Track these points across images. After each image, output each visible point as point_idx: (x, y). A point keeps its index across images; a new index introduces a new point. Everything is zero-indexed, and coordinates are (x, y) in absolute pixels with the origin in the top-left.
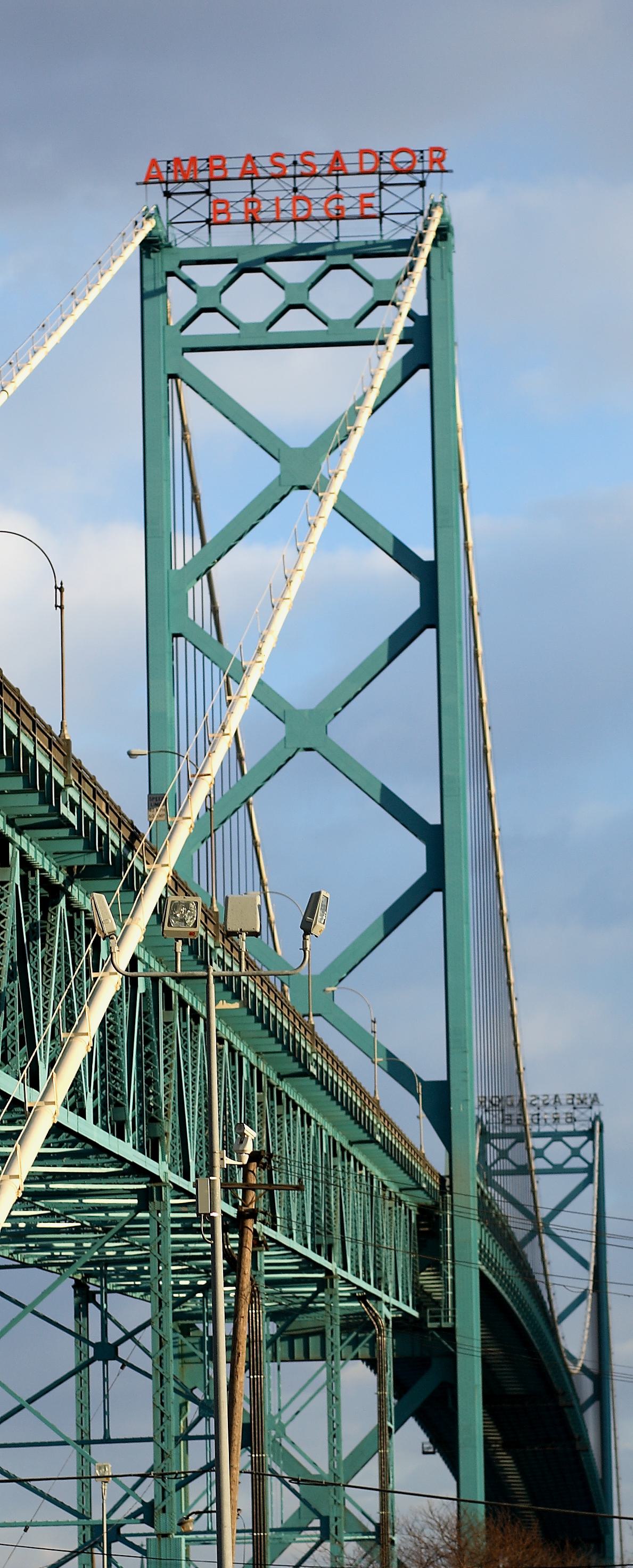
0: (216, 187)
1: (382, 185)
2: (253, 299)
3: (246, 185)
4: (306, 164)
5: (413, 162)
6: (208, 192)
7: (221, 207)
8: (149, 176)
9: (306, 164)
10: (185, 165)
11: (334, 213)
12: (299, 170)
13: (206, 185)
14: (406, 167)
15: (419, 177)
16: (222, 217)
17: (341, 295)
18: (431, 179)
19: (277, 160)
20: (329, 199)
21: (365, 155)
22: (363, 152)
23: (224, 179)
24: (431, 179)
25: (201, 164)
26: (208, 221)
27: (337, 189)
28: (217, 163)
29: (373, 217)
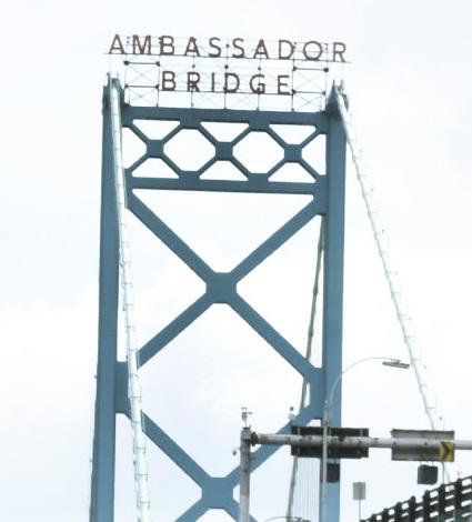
0: (163, 59)
1: (295, 69)
2: (190, 150)
3: (189, 61)
4: (236, 47)
5: (321, 52)
6: (158, 64)
7: (168, 76)
8: (113, 48)
9: (236, 47)
10: (142, 41)
11: (256, 87)
13: (157, 59)
14: (315, 56)
15: (325, 65)
17: (258, 152)
19: (214, 42)
20: (254, 77)
21: (283, 44)
22: (280, 41)
24: (331, 66)
25: (155, 42)
26: (157, 87)
27: (259, 69)
29: (288, 94)
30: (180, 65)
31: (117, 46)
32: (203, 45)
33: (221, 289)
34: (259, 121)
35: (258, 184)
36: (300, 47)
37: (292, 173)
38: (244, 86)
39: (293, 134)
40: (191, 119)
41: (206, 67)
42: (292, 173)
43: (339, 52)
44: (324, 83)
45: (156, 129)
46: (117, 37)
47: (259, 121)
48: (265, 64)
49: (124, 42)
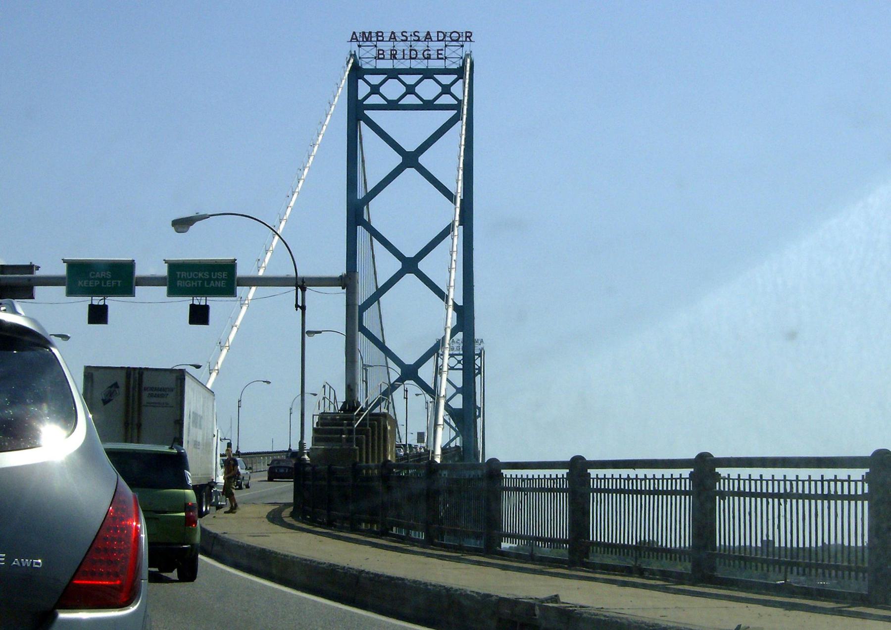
2: (393, 89)
7: (381, 52)
8: (352, 38)
12: (413, 38)
16: (381, 56)
17: (428, 89)
18: (466, 45)
23: (382, 41)
24: (466, 45)
28: (380, 34)
30: (386, 46)
31: (354, 38)
32: (398, 34)
33: (410, 160)
34: (428, 74)
35: (428, 105)
36: (448, 34)
37: (446, 99)
38: (420, 56)
39: (446, 79)
40: (393, 74)
41: (400, 46)
42: (446, 99)
43: (469, 36)
44: (460, 52)
45: (375, 79)
46: (354, 33)
47: (428, 74)
48: (430, 44)
49: (358, 35)
